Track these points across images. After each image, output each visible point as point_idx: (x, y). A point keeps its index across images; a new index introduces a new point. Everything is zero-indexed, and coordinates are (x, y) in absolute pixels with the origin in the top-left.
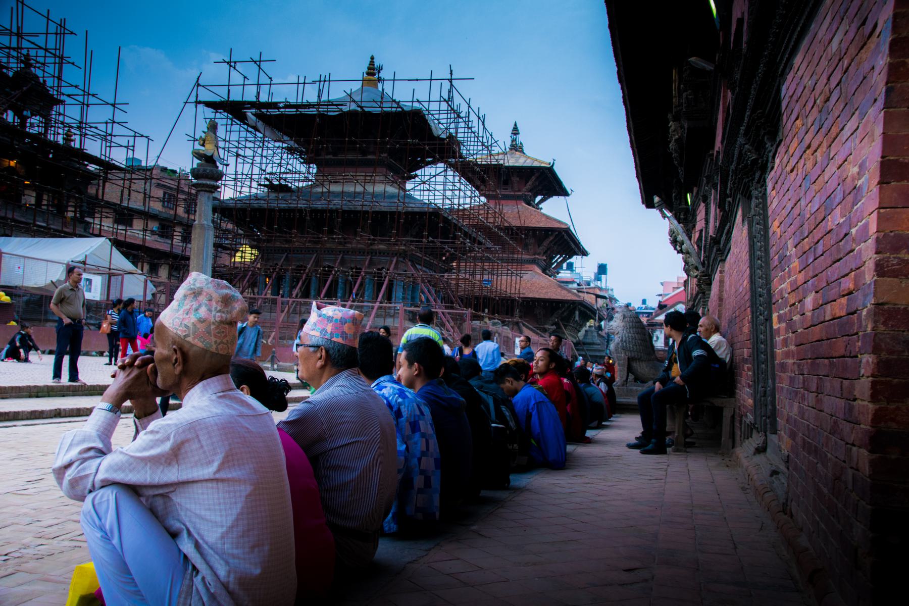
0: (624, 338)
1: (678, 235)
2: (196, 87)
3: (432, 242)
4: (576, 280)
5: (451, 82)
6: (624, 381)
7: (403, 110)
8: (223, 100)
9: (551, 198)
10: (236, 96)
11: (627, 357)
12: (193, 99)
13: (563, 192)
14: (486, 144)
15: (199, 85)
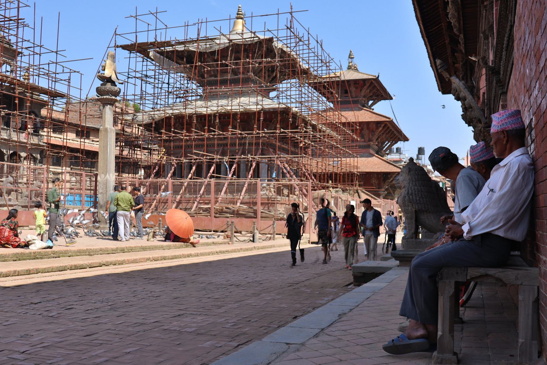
0: (410, 191)
1: (461, 92)
2: (114, 36)
3: (283, 132)
4: (402, 160)
5: (291, 14)
6: (413, 234)
7: (259, 39)
8: (133, 43)
9: (380, 102)
10: (142, 39)
11: (414, 209)
12: (113, 44)
13: (389, 97)
14: (324, 61)
15: (116, 35)
